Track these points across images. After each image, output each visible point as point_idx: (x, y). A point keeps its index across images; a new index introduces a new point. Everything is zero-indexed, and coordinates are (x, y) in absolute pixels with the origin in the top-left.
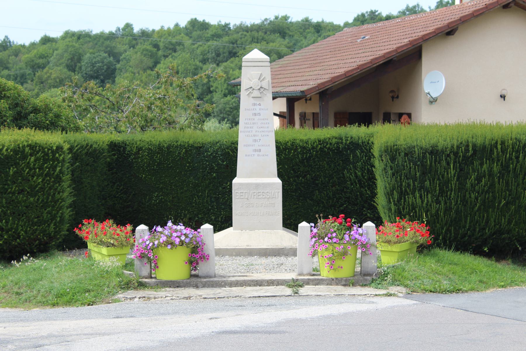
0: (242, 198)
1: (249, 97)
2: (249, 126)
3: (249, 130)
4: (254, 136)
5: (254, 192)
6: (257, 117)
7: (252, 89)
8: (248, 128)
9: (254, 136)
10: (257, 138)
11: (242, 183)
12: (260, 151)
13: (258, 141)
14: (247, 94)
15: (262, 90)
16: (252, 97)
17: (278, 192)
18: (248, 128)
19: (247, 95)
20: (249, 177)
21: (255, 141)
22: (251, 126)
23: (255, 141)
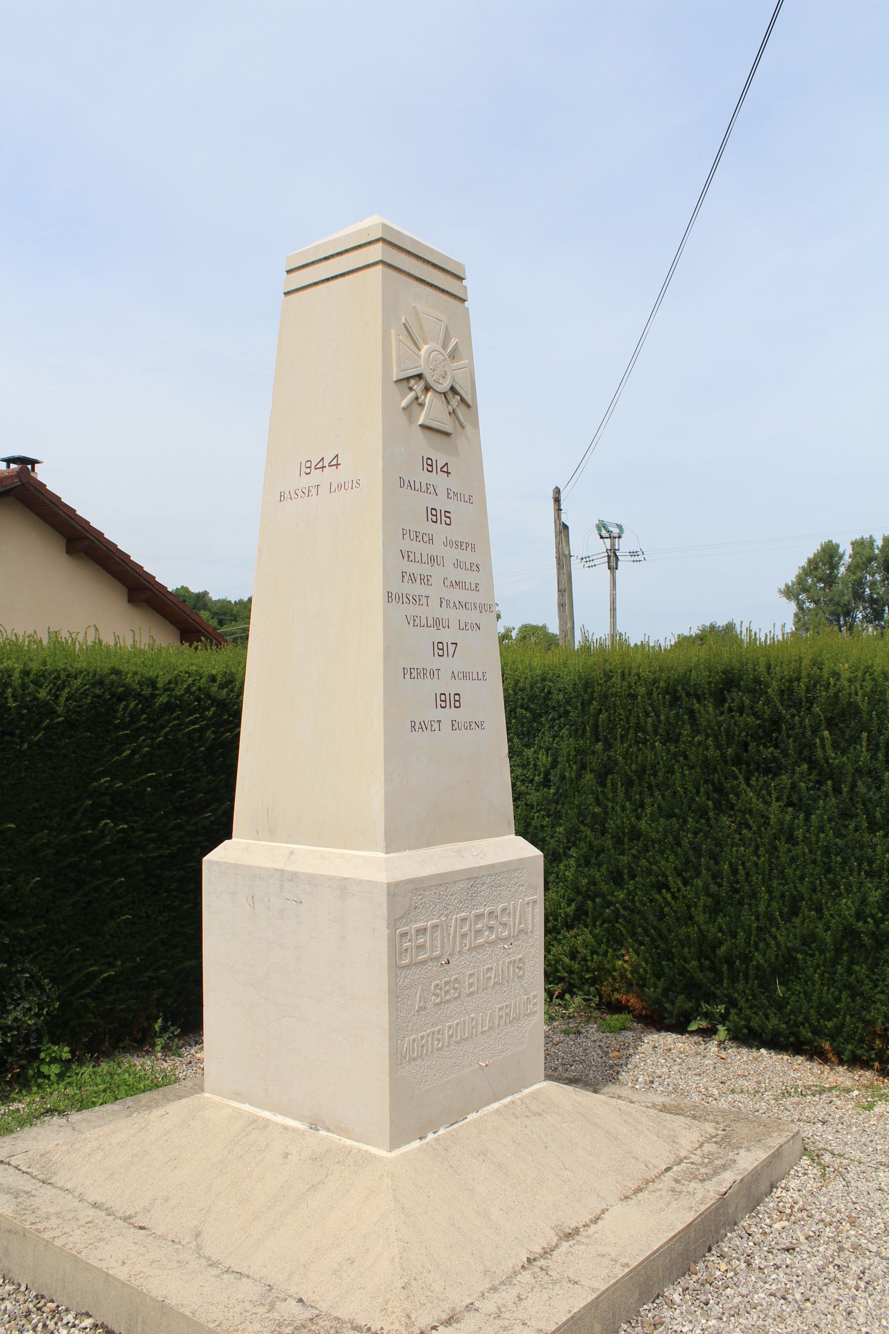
0: (424, 962)
1: (411, 419)
2: (417, 569)
3: (417, 589)
4: (438, 623)
5: (464, 920)
6: (439, 531)
7: (422, 384)
8: (413, 578)
9: (438, 623)
10: (445, 636)
11: (420, 880)
12: (456, 701)
13: (452, 648)
14: (404, 403)
15: (455, 401)
16: (422, 426)
17: (535, 902)
18: (413, 578)
19: (404, 409)
20: (429, 844)
21: (440, 649)
22: (426, 569)
23: (440, 649)
